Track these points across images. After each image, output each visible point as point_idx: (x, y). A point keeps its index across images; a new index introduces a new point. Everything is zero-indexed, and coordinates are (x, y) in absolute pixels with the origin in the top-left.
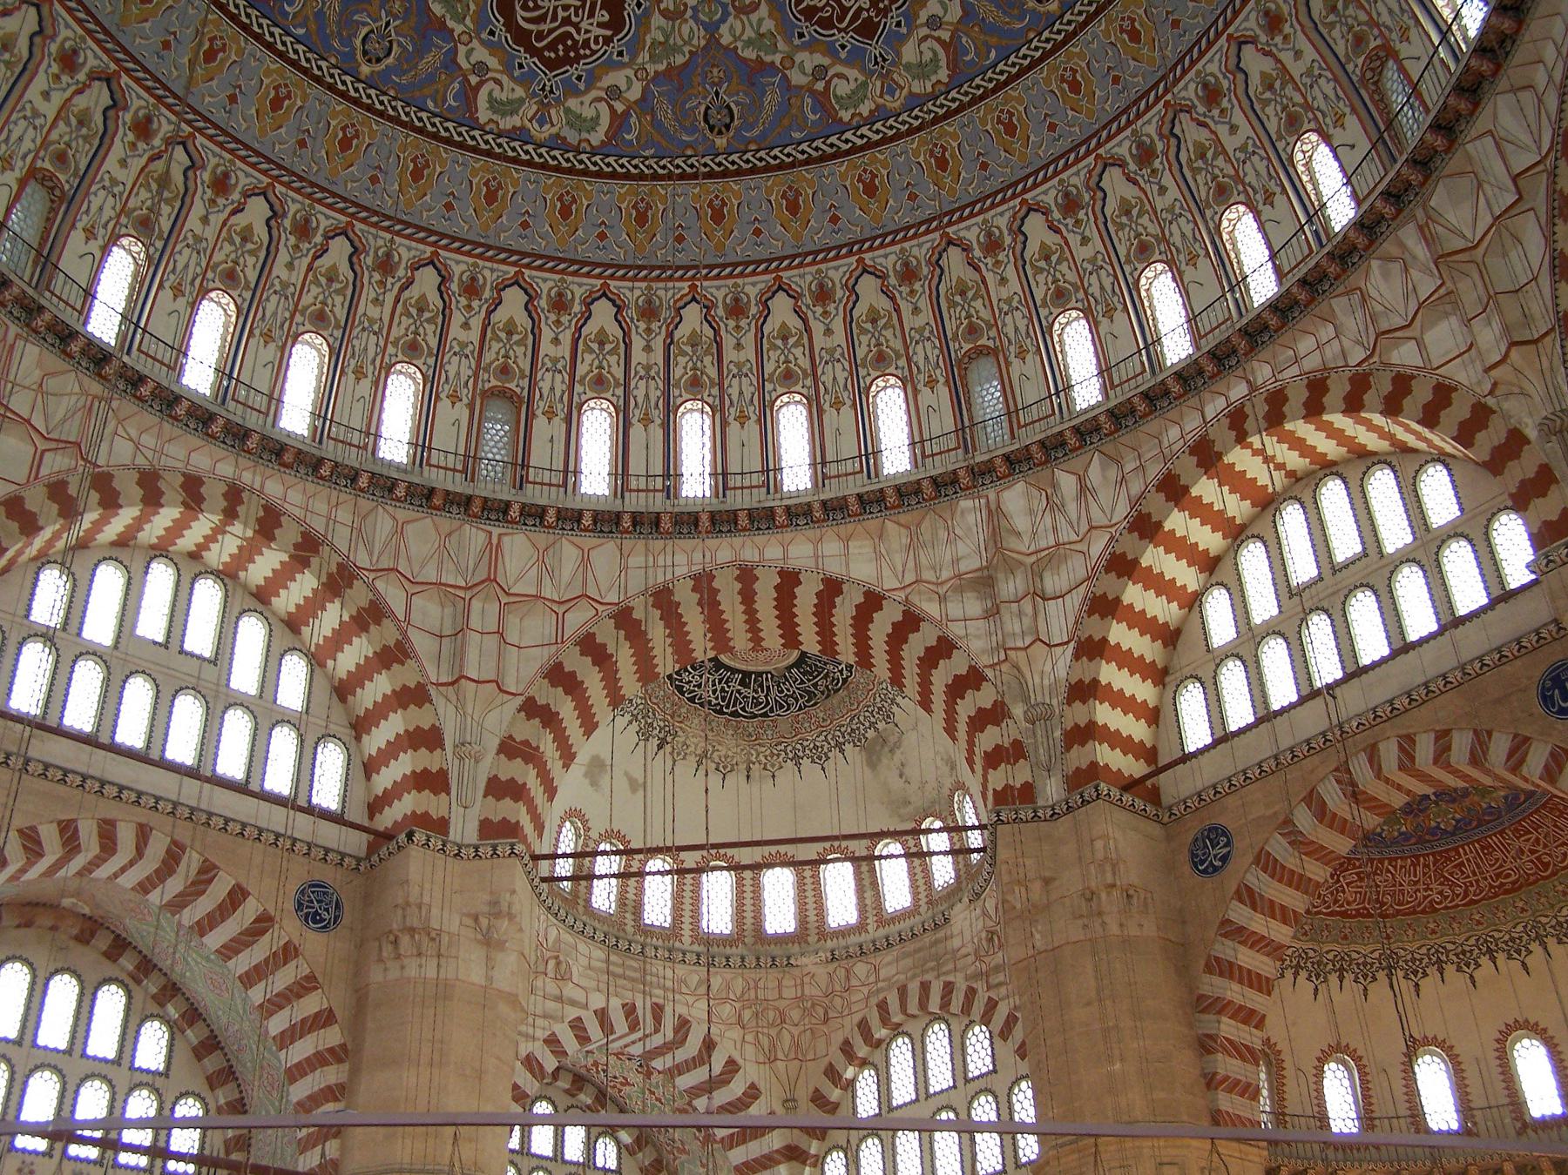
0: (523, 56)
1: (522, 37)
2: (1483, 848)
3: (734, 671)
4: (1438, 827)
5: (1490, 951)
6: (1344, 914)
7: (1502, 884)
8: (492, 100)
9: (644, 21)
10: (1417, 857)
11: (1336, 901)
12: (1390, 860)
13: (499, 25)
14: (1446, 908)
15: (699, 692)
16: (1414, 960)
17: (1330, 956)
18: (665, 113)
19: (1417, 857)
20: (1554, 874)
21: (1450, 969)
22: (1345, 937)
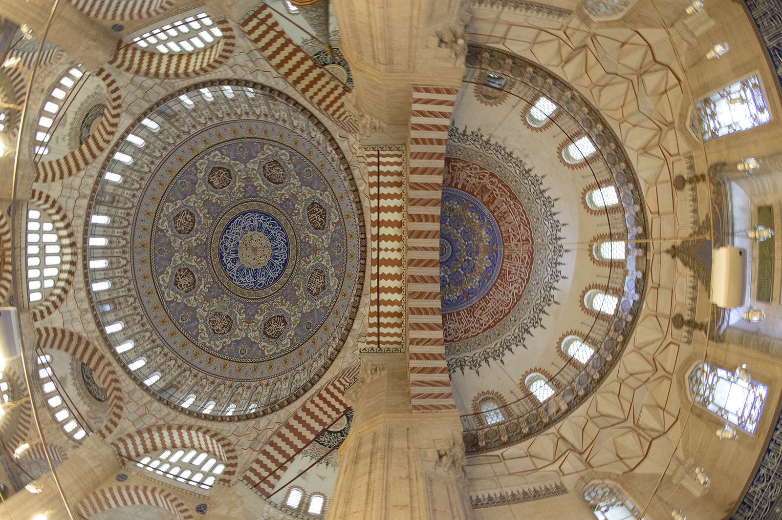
0: (271, 340)
1: (269, 337)
2: (508, 259)
3: (337, 433)
4: (487, 268)
5: (550, 288)
6: (490, 327)
7: (527, 263)
8: (268, 351)
9: (290, 320)
10: (494, 284)
11: (482, 325)
12: (487, 294)
13: (265, 337)
14: (523, 291)
15: (331, 444)
16: (532, 319)
17: (498, 345)
18: (300, 333)
19: (494, 284)
20: (532, 240)
21: (546, 309)
22: (499, 335)
